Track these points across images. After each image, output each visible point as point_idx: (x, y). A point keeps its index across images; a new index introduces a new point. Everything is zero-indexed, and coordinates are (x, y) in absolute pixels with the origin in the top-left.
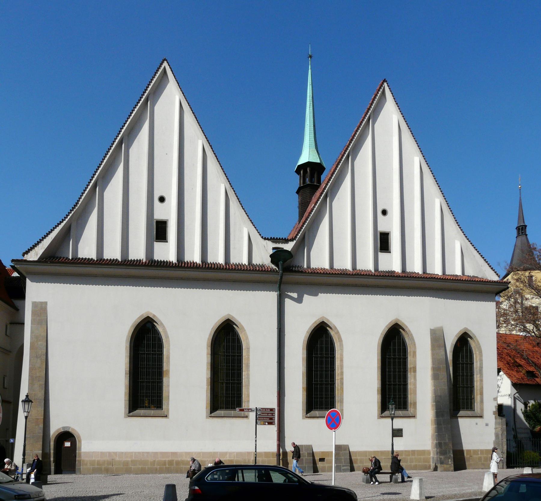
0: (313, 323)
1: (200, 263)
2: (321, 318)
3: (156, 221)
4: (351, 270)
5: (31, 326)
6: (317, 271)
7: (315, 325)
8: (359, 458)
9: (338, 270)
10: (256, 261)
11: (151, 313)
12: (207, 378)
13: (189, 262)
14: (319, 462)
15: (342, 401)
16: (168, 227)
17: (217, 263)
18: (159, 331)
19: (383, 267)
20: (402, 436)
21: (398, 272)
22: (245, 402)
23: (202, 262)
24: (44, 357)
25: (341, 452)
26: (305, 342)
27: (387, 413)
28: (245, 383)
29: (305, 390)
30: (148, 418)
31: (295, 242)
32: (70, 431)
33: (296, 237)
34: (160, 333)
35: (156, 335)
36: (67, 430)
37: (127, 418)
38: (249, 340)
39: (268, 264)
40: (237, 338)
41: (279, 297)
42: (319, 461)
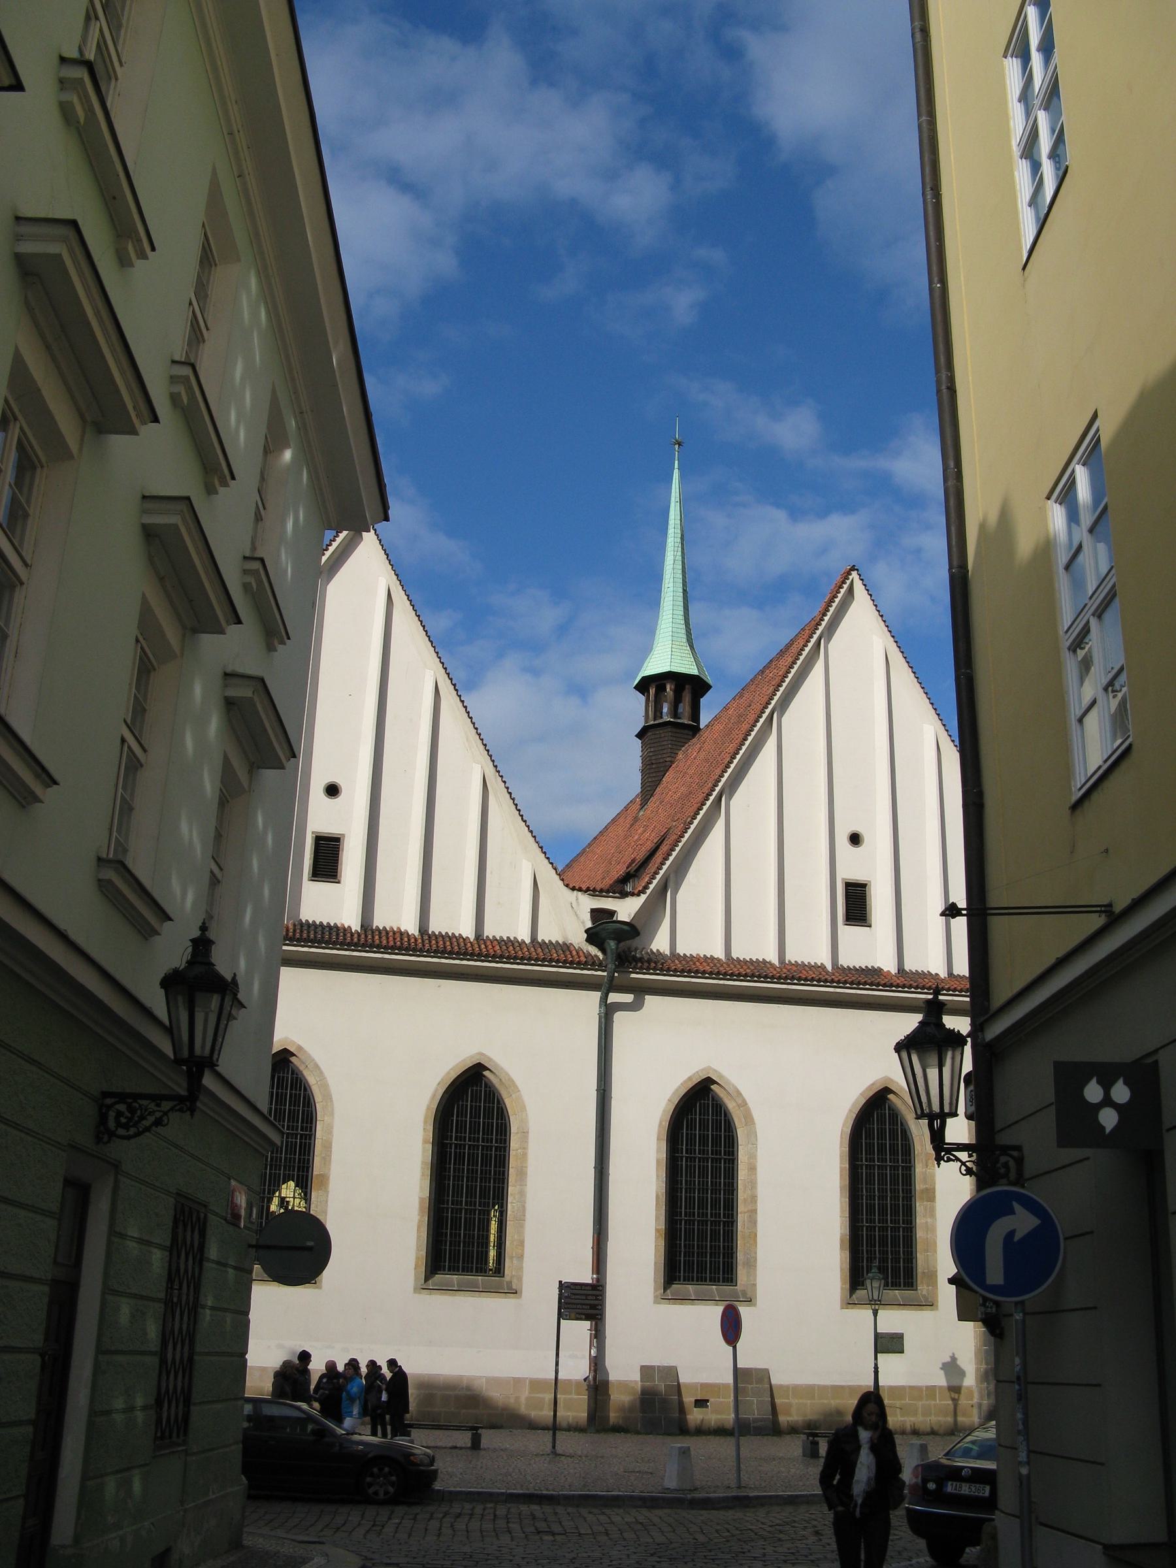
0: (685, 1082)
1: (417, 934)
2: (703, 1070)
4: (777, 964)
6: (694, 964)
7: (690, 1085)
8: (795, 1401)
9: (745, 961)
10: (549, 933)
12: (420, 1198)
13: (388, 929)
14: (695, 1409)
15: (751, 1264)
16: (343, 850)
17: (457, 935)
18: (307, 1082)
19: (848, 959)
20: (902, 1352)
21: (889, 971)
22: (513, 1257)
23: (420, 931)
25: (749, 1386)
26: (664, 1123)
27: (861, 1293)
28: (513, 1212)
29: (661, 1235)
31: (643, 897)
33: (646, 887)
34: (310, 1087)
35: (300, 1090)
39: (578, 944)
40: (498, 1108)
41: (603, 1020)
42: (695, 1407)
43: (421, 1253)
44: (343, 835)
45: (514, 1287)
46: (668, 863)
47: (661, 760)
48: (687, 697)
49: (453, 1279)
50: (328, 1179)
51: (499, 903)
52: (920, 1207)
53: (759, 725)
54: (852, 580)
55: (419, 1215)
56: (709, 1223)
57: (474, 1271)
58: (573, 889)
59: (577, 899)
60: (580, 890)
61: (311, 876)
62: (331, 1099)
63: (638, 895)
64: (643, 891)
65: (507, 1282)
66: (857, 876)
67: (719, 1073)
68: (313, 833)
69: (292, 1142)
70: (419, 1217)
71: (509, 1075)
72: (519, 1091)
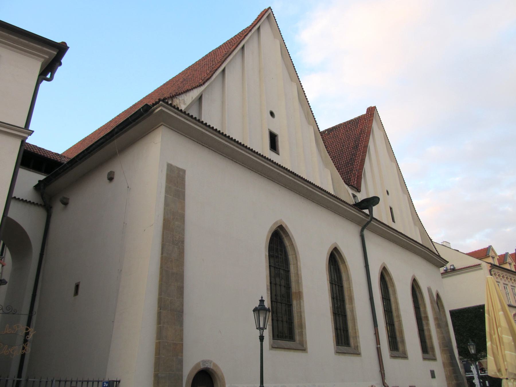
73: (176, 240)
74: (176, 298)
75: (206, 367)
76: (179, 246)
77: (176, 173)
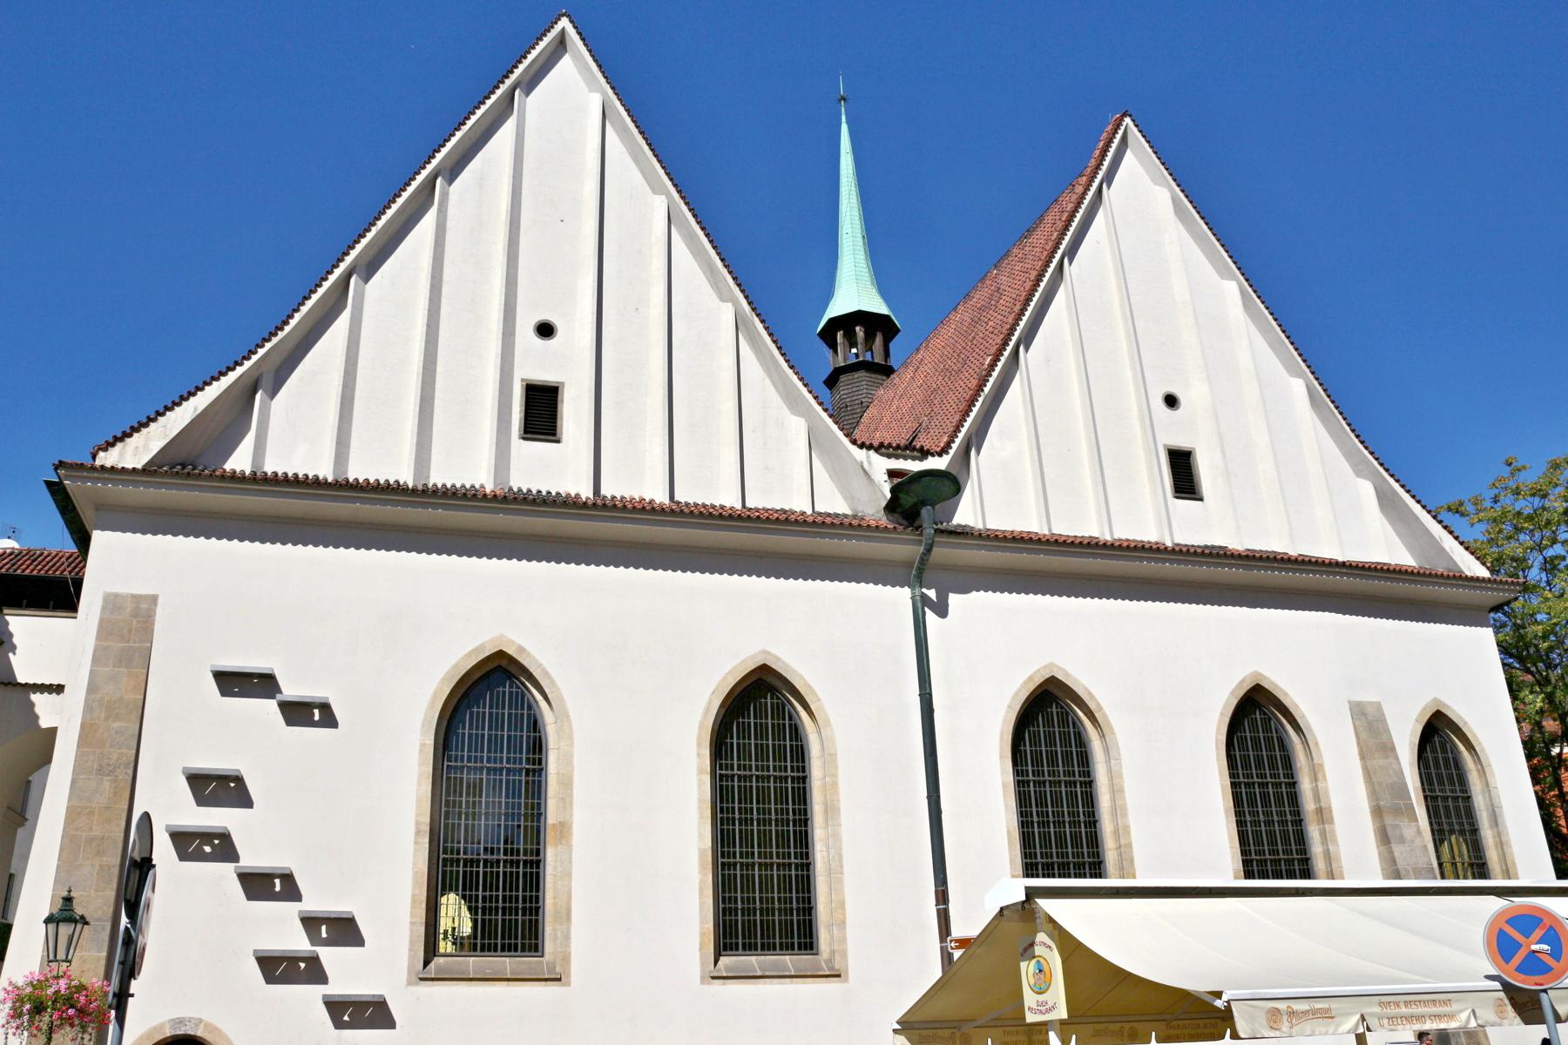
3: (527, 385)
5: (91, 671)
11: (513, 642)
12: (699, 849)
24: (126, 773)
30: (494, 985)
32: (198, 1035)
33: (948, 446)
35: (523, 709)
36: (191, 1033)
37: (416, 984)
38: (832, 730)
43: (706, 926)
44: (563, 384)
45: (837, 967)
46: (970, 420)
47: (857, 402)
48: (879, 340)
49: (751, 961)
50: (570, 827)
51: (767, 468)
52: (1313, 831)
53: (1048, 275)
54: (1126, 127)
55: (699, 873)
56: (1072, 866)
57: (759, 949)
58: (862, 446)
59: (868, 457)
60: (870, 447)
61: (522, 432)
62: (568, 717)
63: (940, 455)
64: (947, 453)
65: (825, 961)
66: (1182, 443)
67: (1064, 670)
68: (522, 380)
69: (514, 781)
70: (700, 876)
71: (804, 679)
72: (819, 700)
73: (109, 765)
74: (93, 891)
75: (182, 1033)
76: (117, 776)
77: (128, 610)
